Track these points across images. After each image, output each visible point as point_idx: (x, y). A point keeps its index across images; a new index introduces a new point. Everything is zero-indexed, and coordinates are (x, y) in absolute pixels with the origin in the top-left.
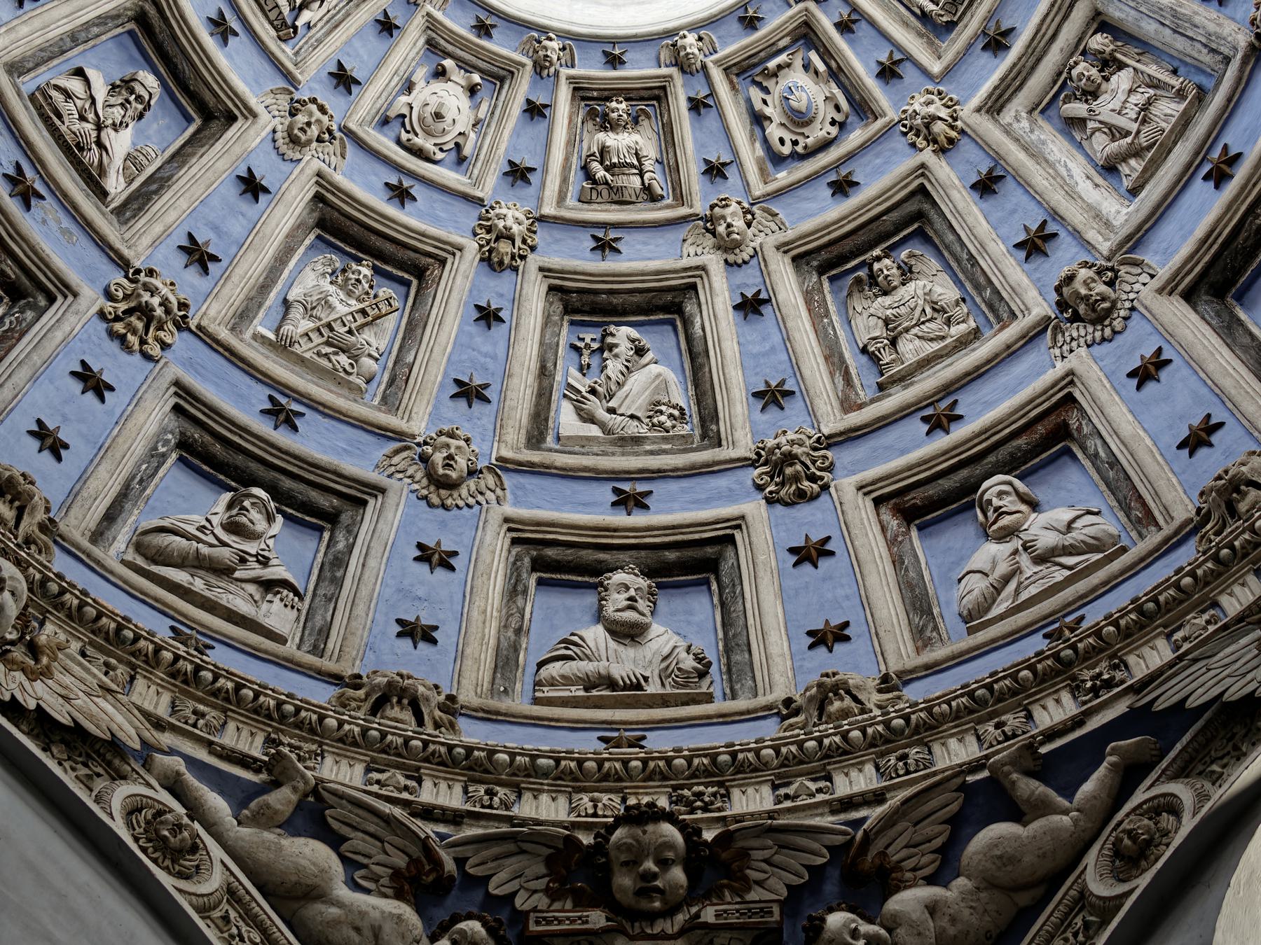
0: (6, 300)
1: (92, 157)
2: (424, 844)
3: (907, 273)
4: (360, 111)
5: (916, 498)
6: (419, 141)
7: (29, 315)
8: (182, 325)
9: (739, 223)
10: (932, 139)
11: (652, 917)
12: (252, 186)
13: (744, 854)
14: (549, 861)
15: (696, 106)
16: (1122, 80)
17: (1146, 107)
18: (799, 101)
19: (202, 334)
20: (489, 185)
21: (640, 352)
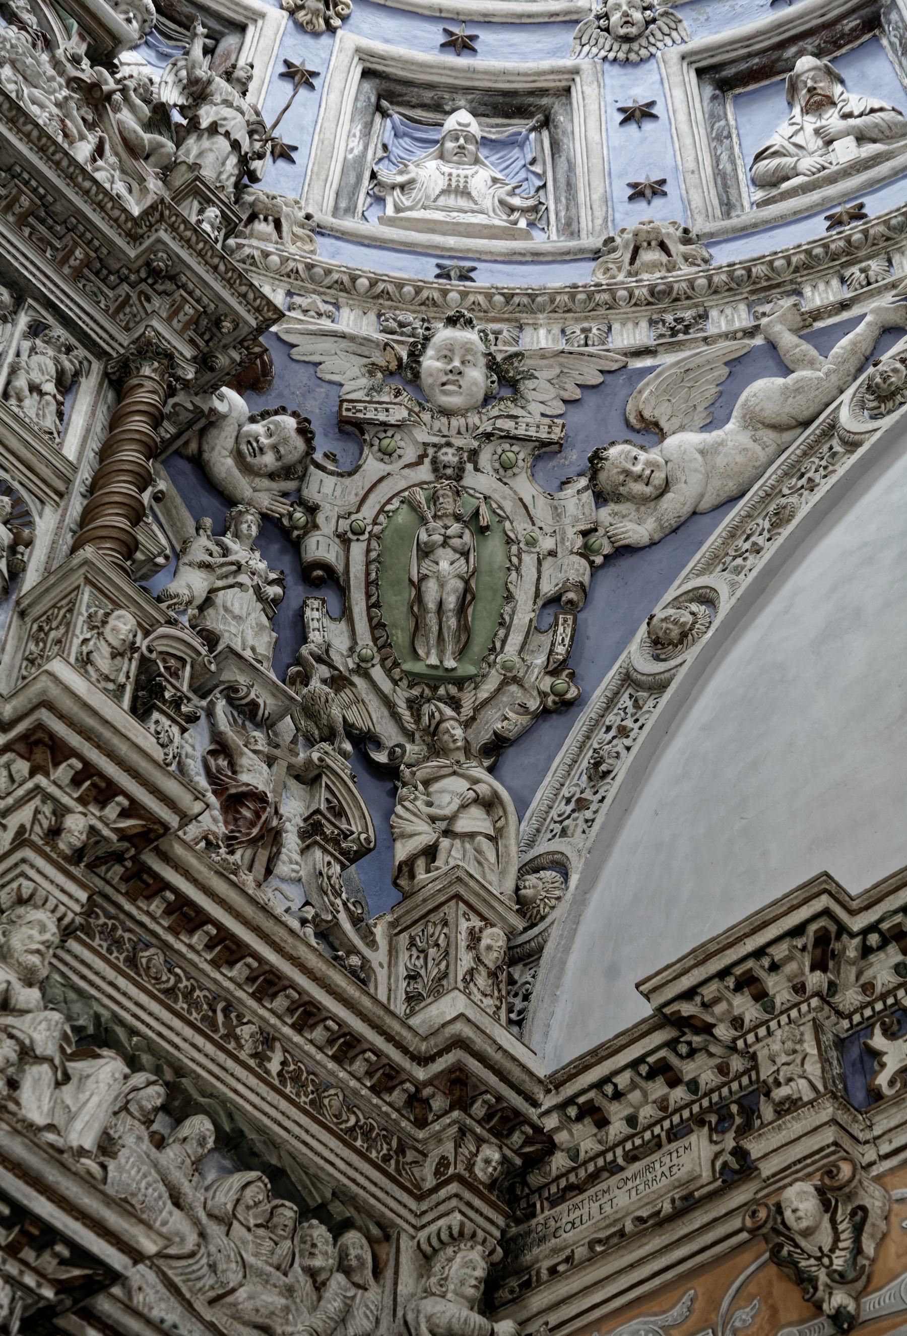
0: (877, 32)
7: (894, 16)
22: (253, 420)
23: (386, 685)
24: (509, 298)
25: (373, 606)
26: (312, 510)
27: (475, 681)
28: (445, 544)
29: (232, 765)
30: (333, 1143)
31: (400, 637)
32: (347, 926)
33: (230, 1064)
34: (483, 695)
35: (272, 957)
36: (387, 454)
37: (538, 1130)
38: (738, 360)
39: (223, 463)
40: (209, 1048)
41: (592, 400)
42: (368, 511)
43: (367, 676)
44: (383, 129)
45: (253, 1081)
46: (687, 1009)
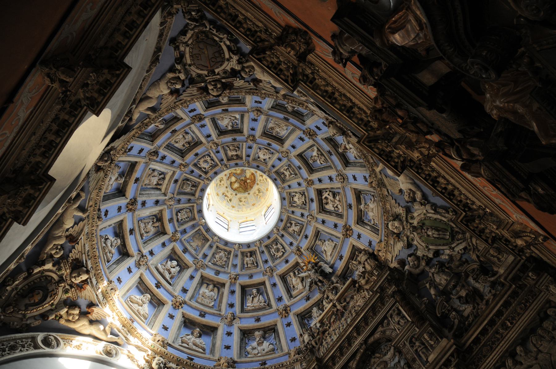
1: (319, 153)
2: (256, 86)
3: (184, 146)
4: (276, 155)
5: (175, 120)
6: (267, 151)
8: (304, 131)
9: (213, 146)
10: (183, 165)
11: (213, 81)
12: (293, 147)
13: (197, 91)
14: (234, 86)
15: (222, 160)
16: (155, 183)
17: (150, 181)
18: (206, 164)
19: (301, 130)
20: (255, 146)
21: (226, 126)
22: (409, 264)
23: (455, 245)
24: (384, 212)
25: (440, 245)
26: (424, 256)
27: (452, 228)
28: (426, 233)
29: (462, 297)
30: (526, 313)
31: (445, 242)
32: (492, 279)
33: (507, 338)
34: (454, 226)
35: (486, 322)
36: (413, 240)
37: (526, 260)
38: (386, 176)
39: (418, 271)
40: (503, 342)
41: (398, 201)
42: (423, 245)
43: (454, 248)
44: (366, 221)
45: (511, 332)
46: (490, 241)
